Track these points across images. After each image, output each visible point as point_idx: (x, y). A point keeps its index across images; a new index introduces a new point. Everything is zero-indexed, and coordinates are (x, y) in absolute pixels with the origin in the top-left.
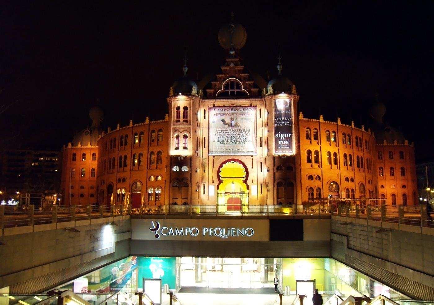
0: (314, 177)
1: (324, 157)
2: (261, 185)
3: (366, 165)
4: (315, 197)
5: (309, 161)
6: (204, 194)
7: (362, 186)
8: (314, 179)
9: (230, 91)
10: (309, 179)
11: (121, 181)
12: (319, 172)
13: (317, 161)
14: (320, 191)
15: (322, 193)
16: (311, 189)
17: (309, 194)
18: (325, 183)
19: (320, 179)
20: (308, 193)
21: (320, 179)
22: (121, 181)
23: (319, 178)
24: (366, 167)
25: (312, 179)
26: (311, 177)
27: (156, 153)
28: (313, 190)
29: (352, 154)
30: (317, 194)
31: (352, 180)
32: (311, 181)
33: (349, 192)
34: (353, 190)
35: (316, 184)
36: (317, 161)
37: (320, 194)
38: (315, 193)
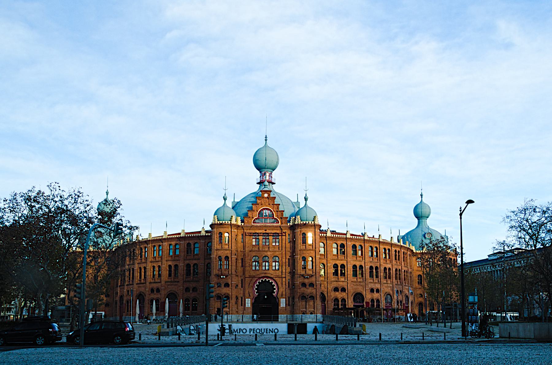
0: (340, 289)
1: (350, 271)
3: (394, 276)
4: (340, 307)
5: (336, 273)
7: (389, 296)
11: (155, 292)
12: (344, 285)
13: (343, 274)
14: (345, 301)
16: (336, 300)
18: (350, 295)
19: (345, 291)
21: (345, 291)
22: (155, 292)
23: (343, 290)
24: (394, 279)
25: (338, 291)
26: (336, 289)
27: (192, 265)
28: (338, 301)
29: (379, 266)
30: (342, 305)
31: (378, 291)
32: (337, 293)
33: (374, 302)
35: (340, 295)
36: (343, 274)
37: (345, 305)
38: (340, 303)
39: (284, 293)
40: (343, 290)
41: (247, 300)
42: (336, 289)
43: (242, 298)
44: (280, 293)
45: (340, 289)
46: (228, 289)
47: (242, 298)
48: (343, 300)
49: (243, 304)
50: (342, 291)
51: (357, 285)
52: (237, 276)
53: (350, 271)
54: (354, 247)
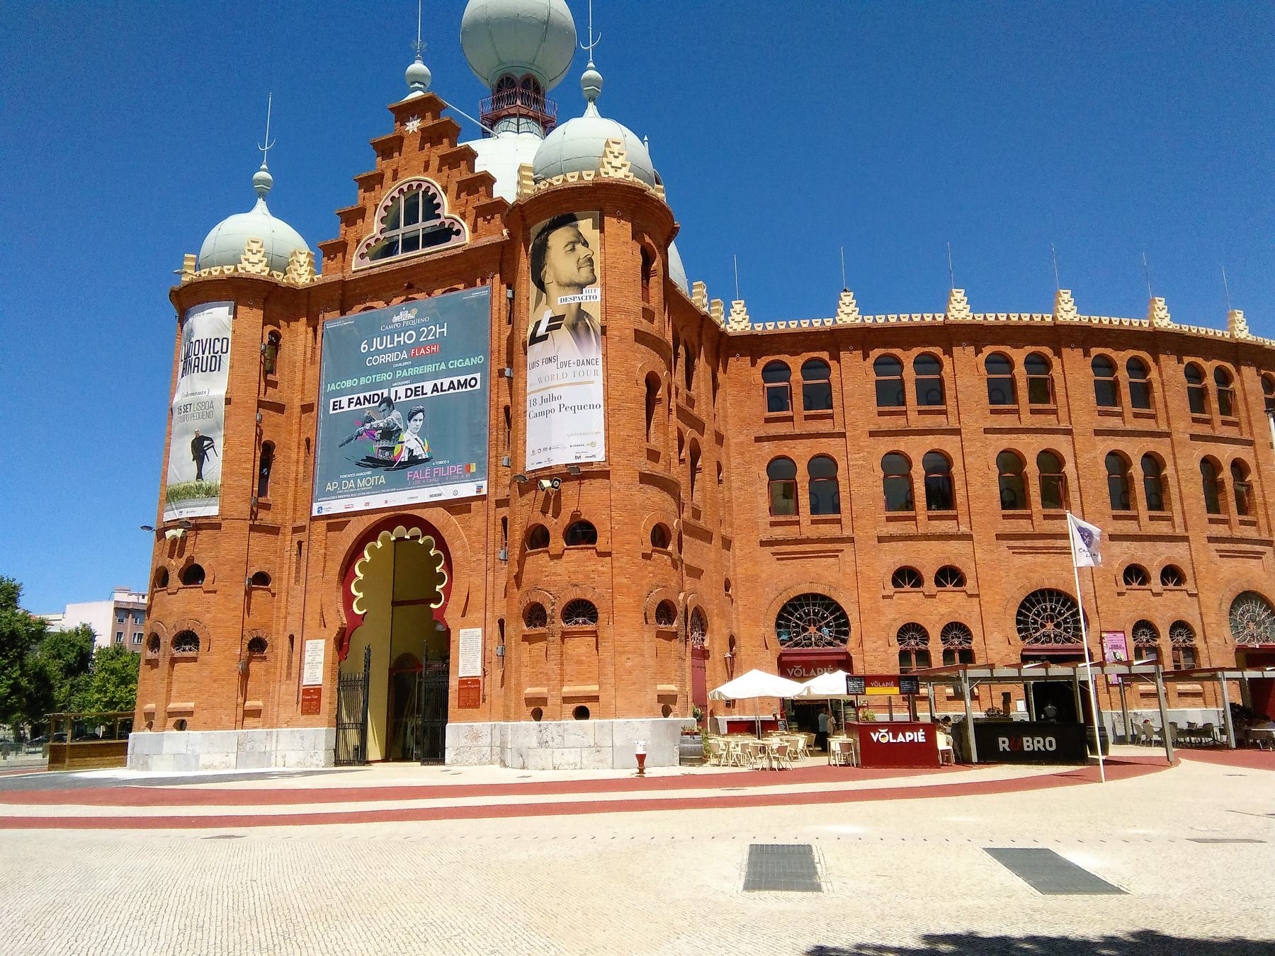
0: (929, 575)
1: (978, 481)
2: (501, 622)
6: (289, 675)
8: (929, 585)
9: (403, 230)
10: (896, 583)
12: (952, 553)
15: (976, 644)
17: (904, 656)
20: (896, 648)
23: (950, 576)
26: (906, 577)
33: (1155, 633)
34: (1180, 627)
35: (936, 608)
38: (936, 648)
39: (477, 598)
40: (950, 576)
41: (309, 644)
42: (906, 577)
43: (292, 638)
44: (457, 598)
45: (929, 575)
46: (192, 593)
47: (292, 638)
48: (955, 629)
49: (295, 666)
50: (938, 583)
51: (1035, 551)
52: (274, 530)
53: (978, 481)
54: (1000, 362)
